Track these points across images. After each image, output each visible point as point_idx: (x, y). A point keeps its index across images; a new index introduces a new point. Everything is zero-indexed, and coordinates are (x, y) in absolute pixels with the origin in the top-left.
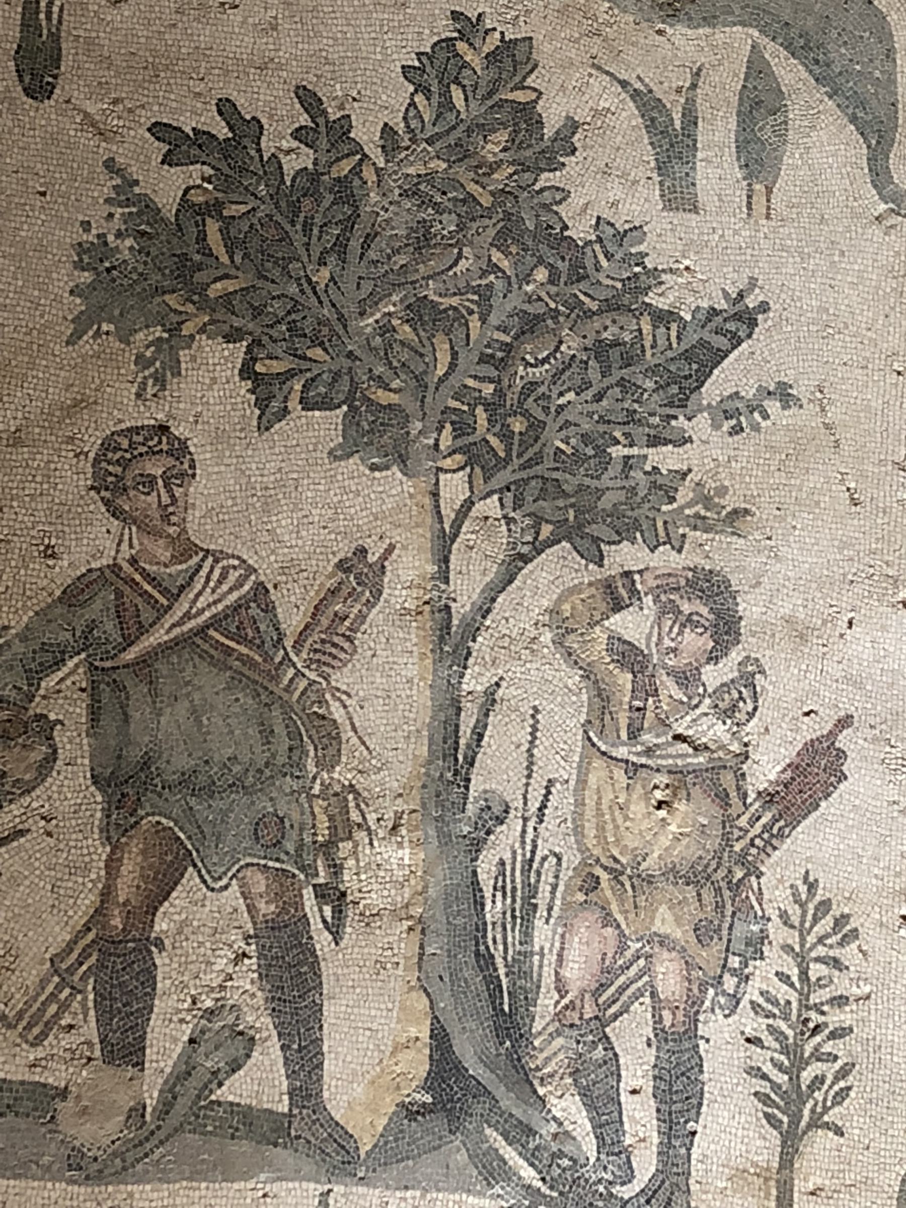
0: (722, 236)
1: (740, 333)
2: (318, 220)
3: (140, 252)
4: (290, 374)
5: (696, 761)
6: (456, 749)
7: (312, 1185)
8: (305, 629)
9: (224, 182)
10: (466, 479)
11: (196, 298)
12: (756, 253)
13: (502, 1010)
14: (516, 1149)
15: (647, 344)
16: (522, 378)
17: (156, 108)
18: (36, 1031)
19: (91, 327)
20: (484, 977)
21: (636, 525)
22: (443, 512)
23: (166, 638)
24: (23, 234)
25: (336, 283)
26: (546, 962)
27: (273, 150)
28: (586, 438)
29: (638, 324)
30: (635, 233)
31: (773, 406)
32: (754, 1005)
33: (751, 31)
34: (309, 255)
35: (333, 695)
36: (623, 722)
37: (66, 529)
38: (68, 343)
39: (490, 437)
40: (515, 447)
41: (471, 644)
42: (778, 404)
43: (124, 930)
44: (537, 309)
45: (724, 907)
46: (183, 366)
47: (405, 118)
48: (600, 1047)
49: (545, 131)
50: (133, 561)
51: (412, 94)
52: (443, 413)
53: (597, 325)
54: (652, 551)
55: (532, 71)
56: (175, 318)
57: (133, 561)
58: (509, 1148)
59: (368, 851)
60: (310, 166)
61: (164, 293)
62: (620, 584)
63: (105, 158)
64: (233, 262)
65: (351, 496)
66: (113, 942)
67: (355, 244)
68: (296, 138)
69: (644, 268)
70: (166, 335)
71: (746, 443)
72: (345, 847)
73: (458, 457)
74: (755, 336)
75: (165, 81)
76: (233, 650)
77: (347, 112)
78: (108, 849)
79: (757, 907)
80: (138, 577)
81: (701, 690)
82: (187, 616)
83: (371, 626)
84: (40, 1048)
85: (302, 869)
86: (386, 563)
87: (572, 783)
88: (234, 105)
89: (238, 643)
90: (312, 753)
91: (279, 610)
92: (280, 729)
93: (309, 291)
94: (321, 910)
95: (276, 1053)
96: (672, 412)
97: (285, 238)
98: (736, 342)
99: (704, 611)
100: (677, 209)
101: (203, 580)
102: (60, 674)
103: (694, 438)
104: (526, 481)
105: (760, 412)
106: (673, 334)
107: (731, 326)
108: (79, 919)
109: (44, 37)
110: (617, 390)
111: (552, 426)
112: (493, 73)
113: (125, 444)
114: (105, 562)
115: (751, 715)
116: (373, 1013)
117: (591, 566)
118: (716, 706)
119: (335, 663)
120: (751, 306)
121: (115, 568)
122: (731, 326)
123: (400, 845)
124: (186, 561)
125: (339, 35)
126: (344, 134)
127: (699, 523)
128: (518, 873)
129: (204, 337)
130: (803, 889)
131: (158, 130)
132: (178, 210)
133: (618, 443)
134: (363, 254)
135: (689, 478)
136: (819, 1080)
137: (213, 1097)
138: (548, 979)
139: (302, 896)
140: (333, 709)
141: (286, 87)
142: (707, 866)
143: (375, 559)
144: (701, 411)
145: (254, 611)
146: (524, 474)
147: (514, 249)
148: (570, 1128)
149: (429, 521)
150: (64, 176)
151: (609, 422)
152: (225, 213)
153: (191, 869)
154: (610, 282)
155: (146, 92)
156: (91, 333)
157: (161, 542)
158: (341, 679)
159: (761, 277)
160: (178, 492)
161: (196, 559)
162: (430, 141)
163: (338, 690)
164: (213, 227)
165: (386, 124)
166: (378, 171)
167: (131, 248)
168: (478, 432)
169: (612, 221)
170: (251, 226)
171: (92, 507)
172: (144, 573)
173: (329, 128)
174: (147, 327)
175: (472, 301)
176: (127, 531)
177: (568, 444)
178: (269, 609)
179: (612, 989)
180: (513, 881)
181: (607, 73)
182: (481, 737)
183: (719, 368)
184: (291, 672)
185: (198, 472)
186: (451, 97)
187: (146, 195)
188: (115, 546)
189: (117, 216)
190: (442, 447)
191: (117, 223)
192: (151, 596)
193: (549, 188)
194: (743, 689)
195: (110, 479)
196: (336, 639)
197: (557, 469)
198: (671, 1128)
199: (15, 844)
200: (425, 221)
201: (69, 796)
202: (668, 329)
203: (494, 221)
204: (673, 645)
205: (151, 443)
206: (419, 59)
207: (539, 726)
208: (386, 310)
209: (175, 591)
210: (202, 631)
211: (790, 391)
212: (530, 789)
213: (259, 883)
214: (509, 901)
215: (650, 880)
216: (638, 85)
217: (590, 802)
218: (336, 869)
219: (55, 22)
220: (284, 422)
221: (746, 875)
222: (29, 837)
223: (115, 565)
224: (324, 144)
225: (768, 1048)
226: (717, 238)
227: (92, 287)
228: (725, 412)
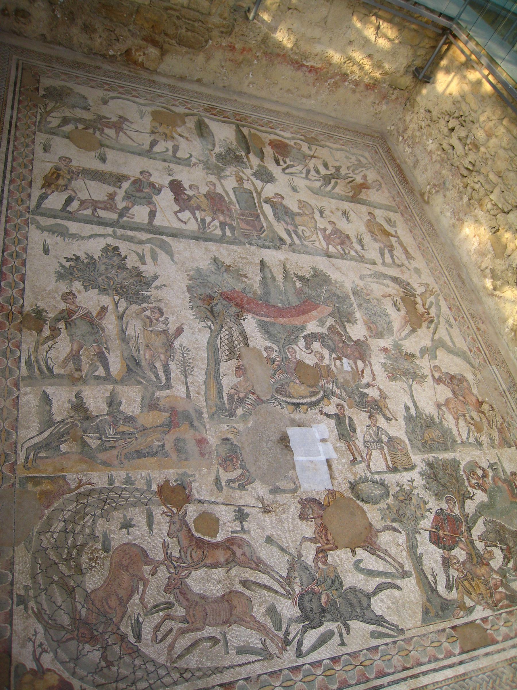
71: (160, 292)
72: (108, 343)
95: (102, 368)
136: (188, 369)
158: (103, 322)
210: (81, 317)
213: (96, 347)
218: (107, 345)
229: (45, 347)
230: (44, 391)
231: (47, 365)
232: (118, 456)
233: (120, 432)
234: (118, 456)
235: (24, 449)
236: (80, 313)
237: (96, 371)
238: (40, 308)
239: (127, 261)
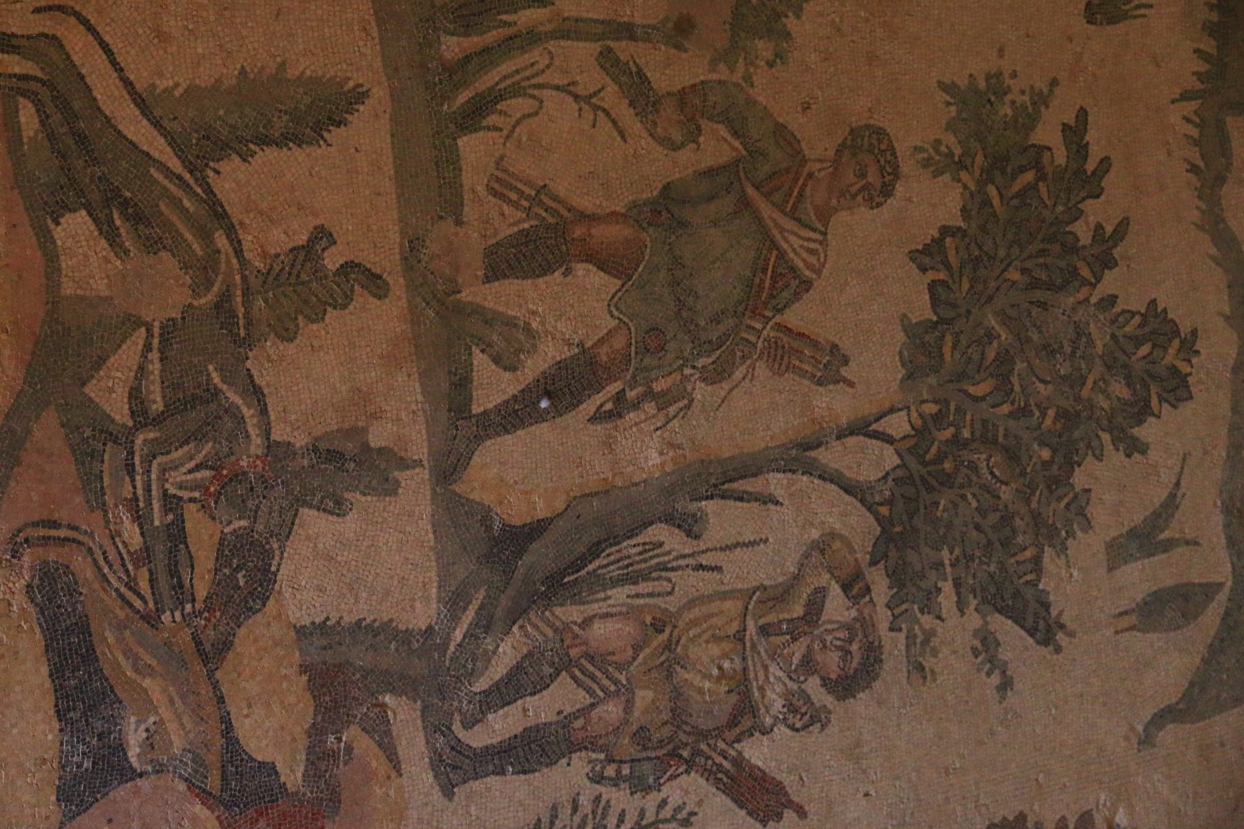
1: (1039, 634)
2: (1049, 260)
3: (1005, 122)
5: (755, 690)
6: (730, 481)
7: (426, 450)
13: (565, 577)
14: (474, 619)
15: (1018, 558)
16: (979, 459)
18: (497, 186)
20: (584, 554)
21: (902, 586)
23: (766, 216)
26: (601, 604)
28: (949, 526)
31: (995, 679)
32: (598, 799)
33: (1231, 578)
36: (771, 618)
41: (800, 472)
43: (573, 239)
44: (1024, 460)
45: (662, 748)
47: (1124, 311)
48: (552, 670)
50: (810, 175)
51: (1139, 312)
52: (945, 400)
53: (1024, 510)
56: (968, 162)
57: (810, 175)
58: (473, 614)
59: (652, 428)
60: (1081, 244)
64: (1012, 199)
66: (564, 233)
67: (1038, 295)
69: (1066, 539)
70: (956, 159)
72: (650, 407)
73: (919, 422)
76: (766, 274)
78: (623, 211)
79: (666, 777)
80: (801, 182)
82: (782, 230)
83: (799, 384)
84: (486, 193)
85: (634, 376)
86: (841, 383)
87: (723, 588)
89: (772, 277)
90: (710, 360)
91: (797, 305)
92: (722, 328)
93: (1003, 266)
95: (512, 390)
98: (1032, 632)
99: (854, 665)
100: (1108, 554)
102: (729, 138)
103: (965, 617)
104: (914, 484)
106: (1029, 577)
107: (1042, 625)
109: (1123, 7)
110: (985, 541)
113: (883, 147)
114: (806, 152)
121: (804, 161)
122: (1042, 625)
123: (661, 453)
127: (911, 638)
128: (656, 560)
129: (961, 190)
130: (684, 814)
131: (1082, 114)
135: (938, 621)
137: (474, 348)
138: (595, 608)
139: (615, 381)
142: (686, 723)
145: (794, 284)
146: (917, 479)
148: (493, 662)
149: (875, 411)
151: (963, 541)
152: (1040, 184)
153: (620, 283)
156: (948, 98)
158: (762, 369)
159: (1077, 640)
160: (860, 198)
162: (1113, 336)
163: (754, 369)
164: (1029, 176)
166: (1087, 300)
167: (1006, 115)
168: (937, 433)
171: (840, 132)
172: (804, 185)
176: (829, 164)
177: (944, 511)
178: (797, 295)
179: (591, 668)
180: (651, 558)
181: (1182, 468)
182: (741, 499)
184: (758, 326)
185: (875, 211)
189: (1024, 98)
191: (1020, 99)
192: (791, 195)
194: (809, 715)
195: (859, 140)
196: (786, 358)
197: (926, 508)
198: (505, 752)
200: (1062, 348)
201: (653, 169)
202: (1031, 572)
204: (828, 643)
207: (756, 546)
208: (1002, 333)
209: (796, 215)
210: (774, 245)
212: (714, 552)
213: (619, 343)
214: (637, 558)
215: (669, 676)
216: (1179, 495)
218: (636, 406)
220: (917, 271)
221: (685, 760)
222: (622, 143)
223: (806, 161)
225: (572, 820)
227: (976, 91)
228: (986, 638)
229: (591, 78)
230: (359, 96)
231: (501, 97)
232: (55, 524)
233: (180, 520)
234: (55, 524)
235: (43, 24)
236: (794, 242)
237: (497, 360)
239: (1115, 457)
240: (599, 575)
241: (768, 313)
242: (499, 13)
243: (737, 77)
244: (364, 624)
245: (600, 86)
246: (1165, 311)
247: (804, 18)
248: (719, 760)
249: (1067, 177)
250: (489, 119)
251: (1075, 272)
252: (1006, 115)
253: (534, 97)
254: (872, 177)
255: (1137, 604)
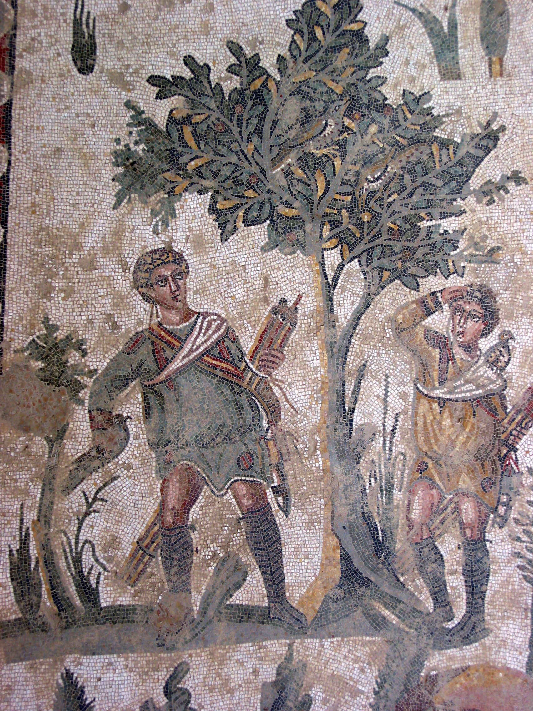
0: (476, 90)
2: (246, 117)
3: (148, 151)
4: (236, 208)
5: (477, 392)
6: (344, 404)
8: (256, 349)
9: (192, 104)
10: (339, 252)
11: (181, 172)
12: (496, 97)
13: (379, 540)
14: (389, 611)
15: (437, 159)
17: (150, 67)
19: (125, 198)
22: (327, 273)
23: (181, 364)
24: (85, 151)
25: (258, 151)
27: (217, 81)
28: (406, 219)
29: (431, 149)
30: (426, 96)
31: (511, 186)
32: (516, 521)
34: (242, 138)
35: (274, 384)
37: (123, 312)
38: (114, 208)
39: (350, 227)
40: (365, 230)
42: (513, 184)
43: (174, 523)
45: (497, 470)
46: (177, 212)
47: (290, 50)
49: (370, 44)
50: (160, 324)
51: (293, 36)
53: (408, 153)
54: (446, 279)
55: (360, 11)
58: (387, 611)
61: (163, 172)
62: (429, 299)
63: (125, 101)
65: (275, 271)
66: (169, 530)
68: (229, 72)
69: (432, 116)
70: (166, 196)
73: (334, 241)
74: (498, 146)
75: (154, 51)
76: (218, 366)
77: (257, 52)
78: (161, 481)
79: (515, 468)
80: (163, 333)
81: (478, 353)
82: (191, 351)
83: (292, 342)
86: (298, 306)
88: (193, 58)
89: (220, 362)
90: (265, 417)
91: (241, 340)
94: (277, 500)
96: (454, 196)
97: (228, 130)
98: (488, 151)
100: (449, 79)
101: (198, 330)
102: (126, 391)
103: (467, 210)
105: (504, 190)
106: (451, 151)
107: (484, 143)
108: (149, 520)
109: (86, 38)
111: (385, 215)
112: (338, 16)
114: (144, 327)
115: (507, 363)
116: (309, 549)
117: (412, 292)
118: (488, 361)
119: (273, 365)
120: (495, 128)
122: (484, 143)
124: (188, 321)
125: (249, 8)
126: (256, 64)
128: (382, 466)
129: (187, 194)
131: (153, 80)
132: (167, 124)
133: (424, 219)
134: (271, 132)
135: (465, 234)
137: (228, 603)
139: (266, 494)
140: (275, 391)
141: (221, 43)
143: (291, 304)
144: (470, 194)
145: (227, 343)
147: (357, 116)
149: (319, 279)
150: (104, 115)
153: (206, 487)
154: (413, 127)
155: (144, 60)
156: (125, 201)
157: (173, 311)
158: (278, 374)
160: (180, 283)
161: (193, 319)
163: (277, 380)
164: (188, 130)
165: (279, 55)
166: (277, 83)
167: (144, 150)
169: (412, 91)
170: (208, 127)
172: (165, 330)
173: (247, 62)
174: (156, 193)
175: (335, 150)
176: (155, 308)
177: (395, 224)
178: (235, 340)
183: (479, 167)
185: (190, 269)
186: (315, 34)
187: (149, 118)
188: (148, 318)
189: (134, 132)
190: (324, 236)
191: (135, 137)
193: (375, 77)
194: (502, 349)
196: (273, 352)
197: (390, 239)
198: (473, 590)
199: (112, 484)
202: (448, 149)
203: (344, 101)
204: (461, 330)
205: (163, 258)
206: (295, 15)
208: (288, 162)
211: (520, 175)
212: (386, 420)
213: (243, 489)
216: (421, 10)
217: (420, 423)
218: (282, 477)
219: (91, 28)
221: (508, 451)
222: (119, 480)
224: (245, 72)
225: (524, 542)
226: (472, 91)
228: (483, 192)
238: (60, 335)
240: (383, 513)
241: (242, 367)
242: (30, 570)
243: (88, 381)
244: (377, 689)
245: (82, 495)
246: (295, 12)
247: (59, 323)
248: (514, 425)
249: (192, 97)
250: (92, 582)
251: (258, 93)
252: (144, 150)
253: (83, 547)
254: (166, 272)
255: (487, 55)
